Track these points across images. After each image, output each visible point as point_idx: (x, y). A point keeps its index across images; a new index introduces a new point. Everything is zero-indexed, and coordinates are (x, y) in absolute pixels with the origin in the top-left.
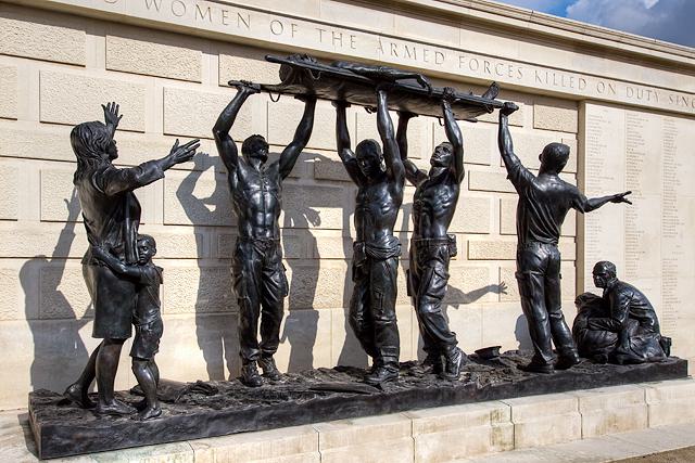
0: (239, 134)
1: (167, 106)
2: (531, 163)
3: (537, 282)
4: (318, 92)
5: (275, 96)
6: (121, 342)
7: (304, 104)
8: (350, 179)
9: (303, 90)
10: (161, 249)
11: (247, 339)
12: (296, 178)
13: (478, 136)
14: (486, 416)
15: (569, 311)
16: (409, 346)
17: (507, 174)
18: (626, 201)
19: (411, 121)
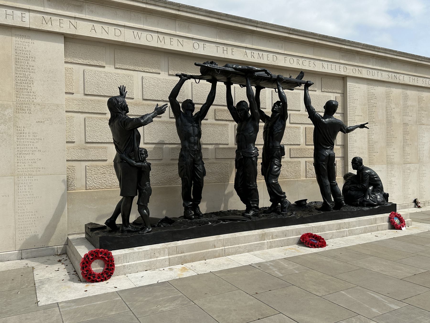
0: (180, 99)
1: (148, 88)
2: (320, 111)
3: (324, 167)
5: (197, 80)
6: (132, 198)
8: (233, 119)
11: (186, 197)
12: (207, 120)
13: (295, 97)
15: (340, 182)
16: (265, 201)
18: (366, 127)
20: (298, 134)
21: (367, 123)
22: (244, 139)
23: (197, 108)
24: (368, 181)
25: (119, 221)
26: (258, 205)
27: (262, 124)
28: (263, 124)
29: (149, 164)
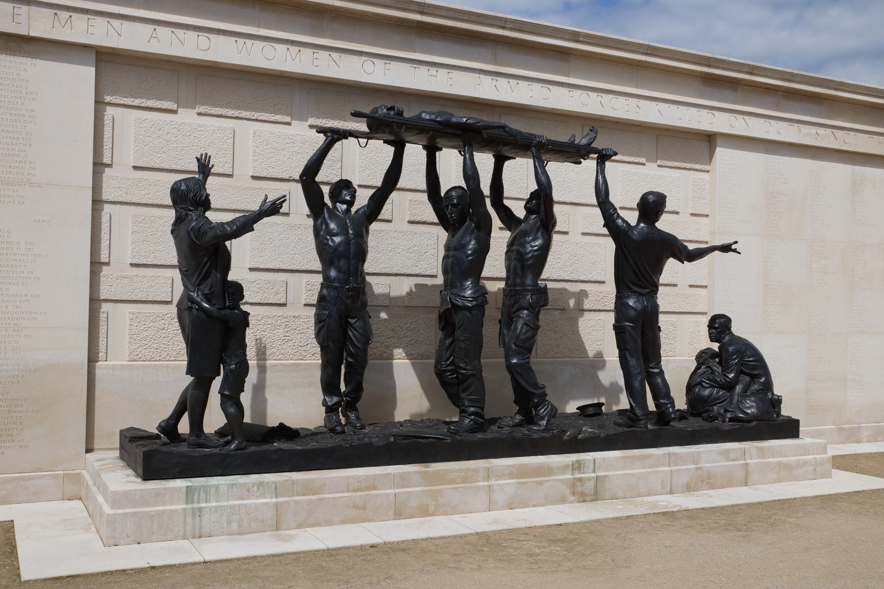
0: (327, 175)
4: (407, 139)
5: (363, 141)
9: (391, 138)
10: (248, 296)
13: (571, 180)
14: (567, 466)
17: (603, 222)
18: (735, 251)
19: (507, 164)
20: (581, 258)
21: (736, 242)
22: (462, 265)
23: (362, 198)
25: (184, 426)
26: (482, 409)
27: (500, 237)
28: (507, 234)
29: (247, 314)
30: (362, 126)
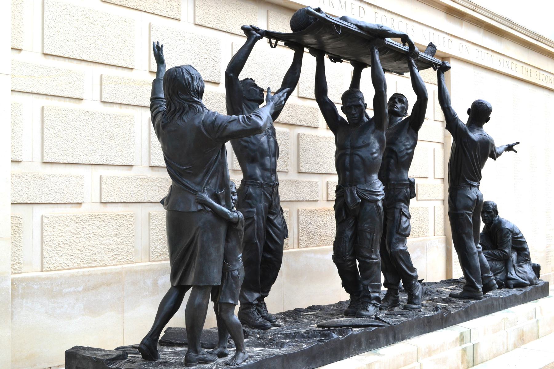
2: (464, 118)
7: (293, 52)
24: (510, 243)
30: (284, 26)
